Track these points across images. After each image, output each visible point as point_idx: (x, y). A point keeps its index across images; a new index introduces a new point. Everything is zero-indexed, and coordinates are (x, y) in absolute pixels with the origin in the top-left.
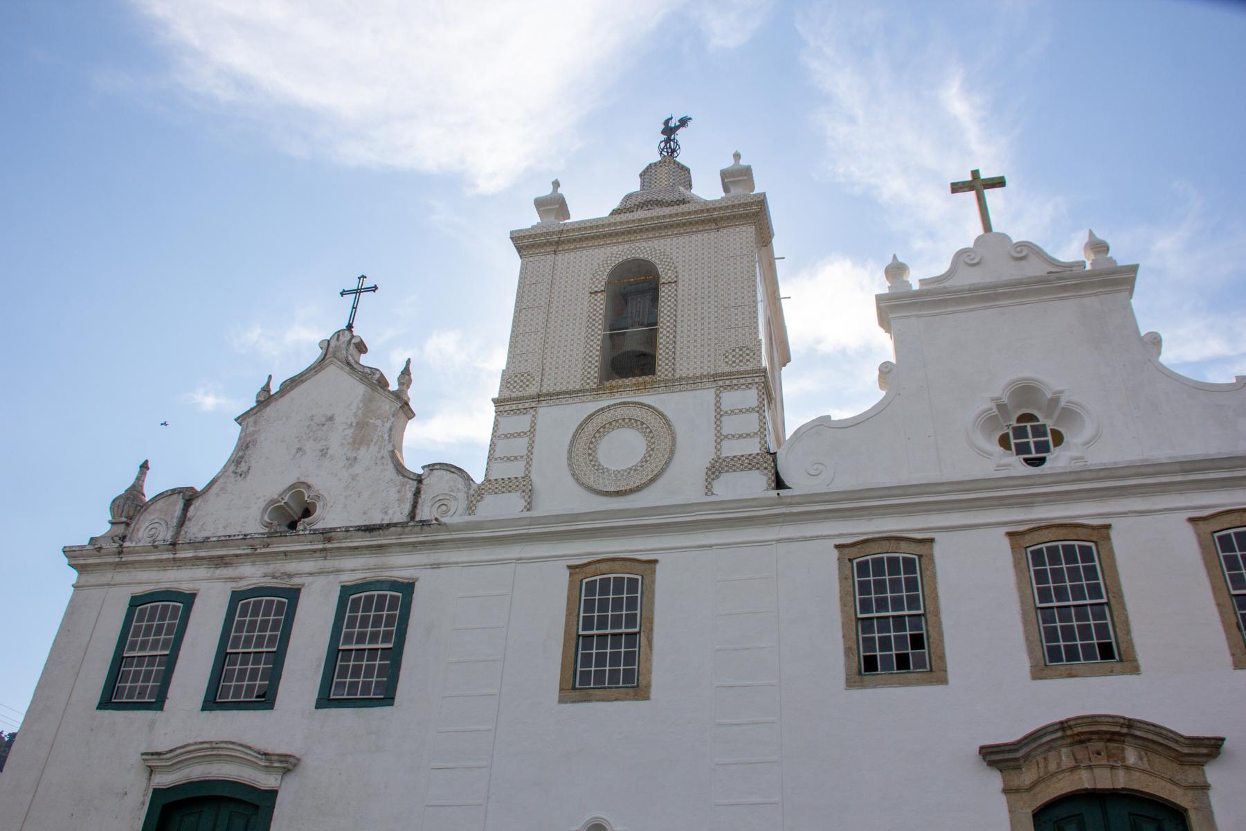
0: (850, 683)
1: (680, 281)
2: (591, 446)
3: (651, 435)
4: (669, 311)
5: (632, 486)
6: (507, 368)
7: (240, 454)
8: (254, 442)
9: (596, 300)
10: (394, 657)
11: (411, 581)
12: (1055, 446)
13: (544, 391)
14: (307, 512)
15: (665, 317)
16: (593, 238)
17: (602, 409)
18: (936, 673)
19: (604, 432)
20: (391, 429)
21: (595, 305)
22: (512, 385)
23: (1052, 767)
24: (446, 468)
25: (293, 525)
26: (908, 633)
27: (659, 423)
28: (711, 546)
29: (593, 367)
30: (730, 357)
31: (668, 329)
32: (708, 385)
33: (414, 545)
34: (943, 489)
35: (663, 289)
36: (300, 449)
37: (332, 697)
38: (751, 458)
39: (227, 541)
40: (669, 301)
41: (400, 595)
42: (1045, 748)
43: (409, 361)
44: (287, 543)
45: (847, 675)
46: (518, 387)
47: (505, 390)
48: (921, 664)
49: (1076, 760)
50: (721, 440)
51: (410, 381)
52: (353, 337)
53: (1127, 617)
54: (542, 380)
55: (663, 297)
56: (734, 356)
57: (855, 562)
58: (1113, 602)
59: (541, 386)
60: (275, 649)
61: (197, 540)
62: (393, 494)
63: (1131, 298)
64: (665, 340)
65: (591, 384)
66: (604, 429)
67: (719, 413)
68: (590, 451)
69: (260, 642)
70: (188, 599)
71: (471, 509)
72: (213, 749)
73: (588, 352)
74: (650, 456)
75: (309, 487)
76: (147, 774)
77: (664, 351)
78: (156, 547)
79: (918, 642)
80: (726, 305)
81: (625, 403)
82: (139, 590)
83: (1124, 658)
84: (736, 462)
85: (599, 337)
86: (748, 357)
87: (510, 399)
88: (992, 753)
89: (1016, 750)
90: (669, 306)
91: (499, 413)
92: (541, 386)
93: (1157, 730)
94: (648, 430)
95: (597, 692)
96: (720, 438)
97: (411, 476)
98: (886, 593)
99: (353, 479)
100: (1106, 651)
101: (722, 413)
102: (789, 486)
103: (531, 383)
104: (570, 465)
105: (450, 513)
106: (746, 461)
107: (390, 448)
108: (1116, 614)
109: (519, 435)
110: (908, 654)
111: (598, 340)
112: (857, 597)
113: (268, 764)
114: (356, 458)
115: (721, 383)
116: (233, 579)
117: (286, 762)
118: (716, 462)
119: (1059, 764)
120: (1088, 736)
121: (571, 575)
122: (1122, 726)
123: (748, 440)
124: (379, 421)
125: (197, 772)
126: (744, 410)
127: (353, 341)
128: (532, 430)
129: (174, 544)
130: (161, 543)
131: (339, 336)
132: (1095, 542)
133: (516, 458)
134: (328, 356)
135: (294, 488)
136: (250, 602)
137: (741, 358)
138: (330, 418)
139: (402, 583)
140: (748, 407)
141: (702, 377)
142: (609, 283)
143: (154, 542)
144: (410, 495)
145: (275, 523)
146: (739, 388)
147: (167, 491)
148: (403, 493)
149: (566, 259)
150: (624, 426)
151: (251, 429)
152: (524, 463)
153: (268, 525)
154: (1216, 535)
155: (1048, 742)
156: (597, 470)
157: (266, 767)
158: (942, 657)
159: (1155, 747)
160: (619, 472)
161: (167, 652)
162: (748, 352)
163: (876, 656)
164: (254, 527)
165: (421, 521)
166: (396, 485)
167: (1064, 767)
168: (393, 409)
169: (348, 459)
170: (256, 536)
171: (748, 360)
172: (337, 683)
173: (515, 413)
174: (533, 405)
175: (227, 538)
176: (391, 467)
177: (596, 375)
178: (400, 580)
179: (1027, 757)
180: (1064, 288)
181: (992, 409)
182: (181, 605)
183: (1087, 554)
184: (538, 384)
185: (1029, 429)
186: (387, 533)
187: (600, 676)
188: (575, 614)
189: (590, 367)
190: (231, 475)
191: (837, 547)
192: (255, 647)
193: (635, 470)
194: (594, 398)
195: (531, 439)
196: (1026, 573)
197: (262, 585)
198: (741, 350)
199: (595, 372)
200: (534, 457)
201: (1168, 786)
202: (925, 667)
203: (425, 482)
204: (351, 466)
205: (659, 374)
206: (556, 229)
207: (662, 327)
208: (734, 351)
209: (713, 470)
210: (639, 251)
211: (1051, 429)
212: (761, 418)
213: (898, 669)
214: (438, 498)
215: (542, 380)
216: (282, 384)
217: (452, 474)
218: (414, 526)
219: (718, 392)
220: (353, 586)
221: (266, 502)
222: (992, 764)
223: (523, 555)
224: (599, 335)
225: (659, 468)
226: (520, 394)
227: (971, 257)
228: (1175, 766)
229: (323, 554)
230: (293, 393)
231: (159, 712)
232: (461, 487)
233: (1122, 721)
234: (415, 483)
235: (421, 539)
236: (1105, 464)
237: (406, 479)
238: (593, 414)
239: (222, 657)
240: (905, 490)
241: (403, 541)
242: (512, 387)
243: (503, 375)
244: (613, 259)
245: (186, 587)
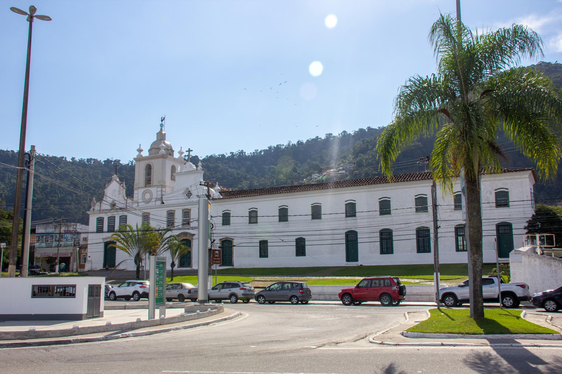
82: (98, 217)
96: (157, 195)
245: (103, 217)
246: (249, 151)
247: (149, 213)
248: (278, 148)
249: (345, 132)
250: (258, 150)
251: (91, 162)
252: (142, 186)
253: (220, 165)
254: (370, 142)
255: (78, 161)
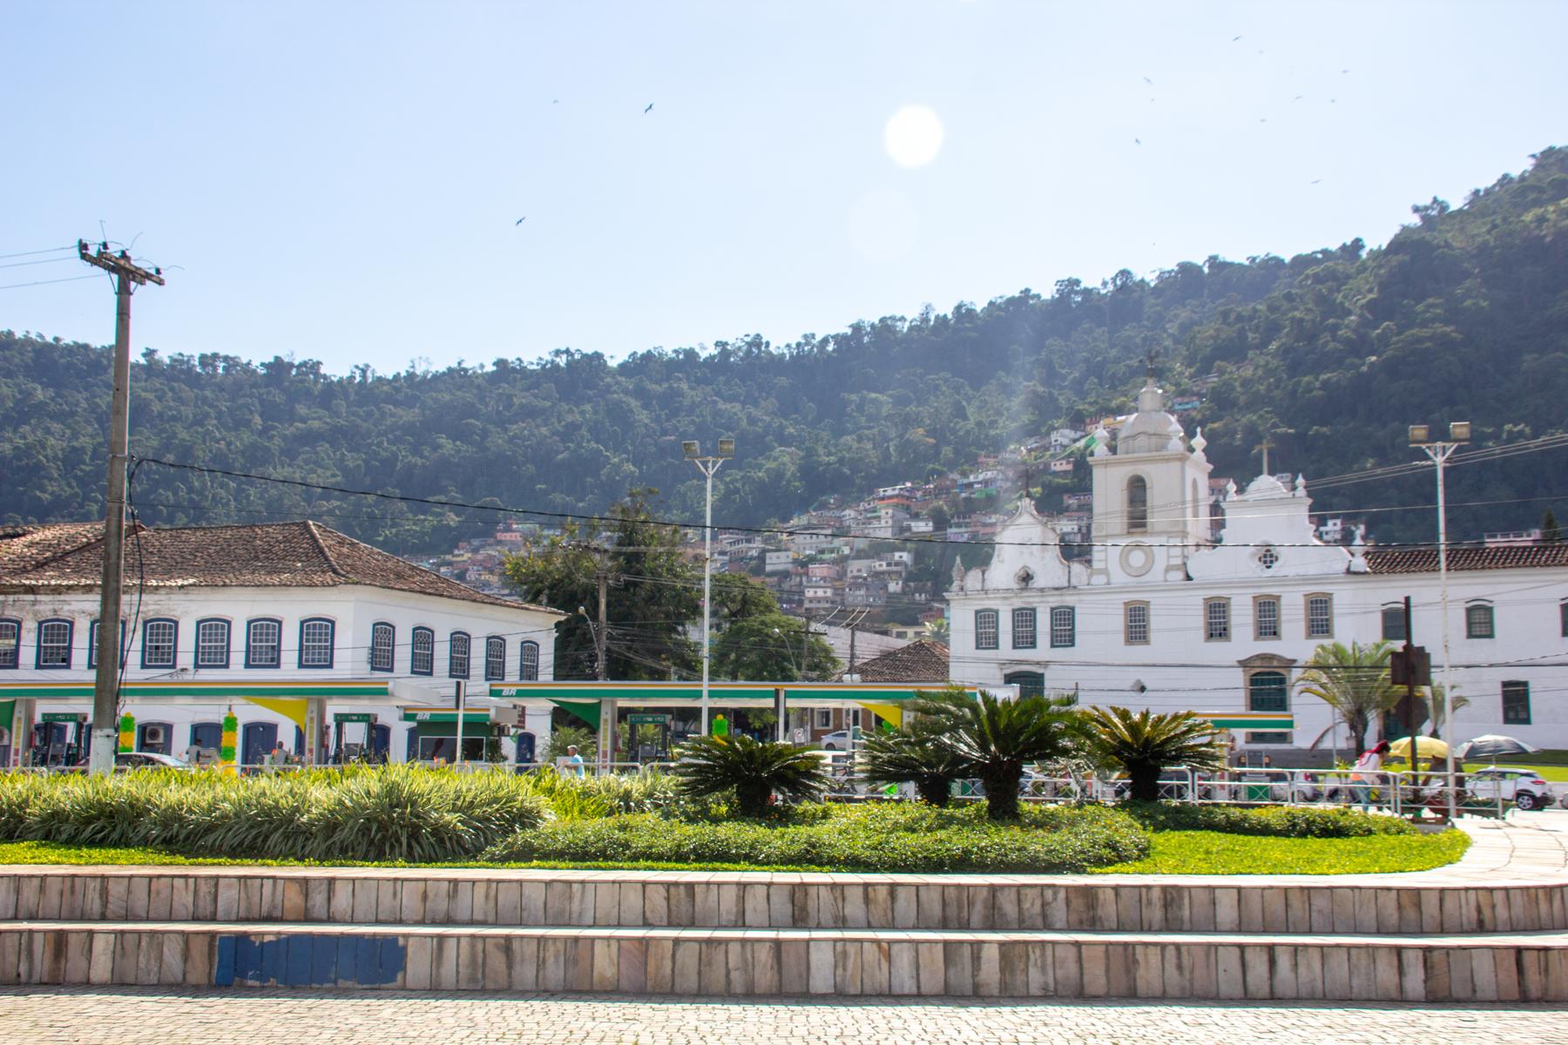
82: (979, 608)
100: (1275, 633)
245: (995, 607)
246: (781, 339)
247: (1148, 603)
248: (885, 328)
249: (1125, 273)
250: (813, 336)
251: (215, 368)
252: (1118, 531)
253: (684, 386)
254: (1251, 318)
255: (167, 361)
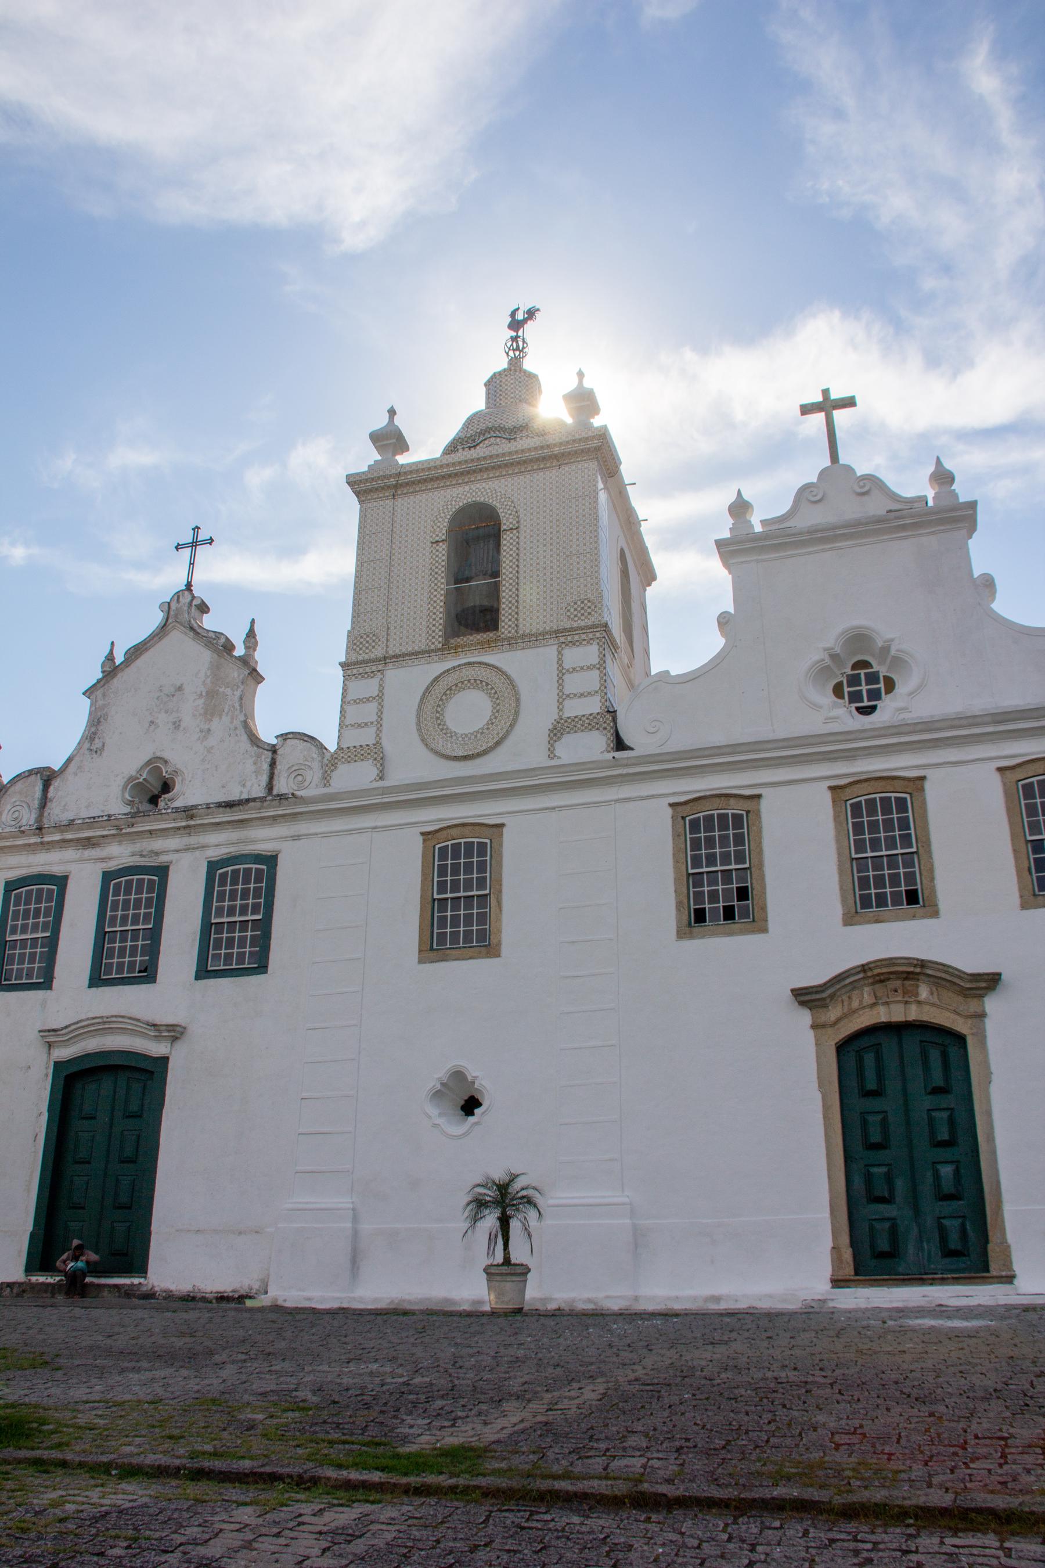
0: (681, 935)
1: (522, 527)
2: (439, 709)
3: (496, 696)
4: (511, 561)
5: (479, 750)
6: (353, 628)
7: (93, 729)
8: (106, 717)
9: (437, 551)
10: (265, 927)
11: (274, 854)
12: (886, 693)
13: (391, 653)
14: (166, 787)
15: (508, 567)
16: (432, 479)
17: (448, 670)
18: (758, 924)
19: (451, 694)
20: (241, 699)
21: (437, 556)
22: (358, 646)
23: (855, 1004)
24: (299, 737)
25: (154, 800)
26: (735, 886)
27: (504, 683)
28: (554, 808)
29: (437, 624)
30: (572, 610)
31: (511, 581)
32: (551, 642)
33: (274, 818)
34: (769, 746)
35: (505, 537)
36: (152, 722)
37: (209, 968)
38: (591, 718)
39: (93, 822)
40: (511, 550)
41: (264, 867)
42: (849, 988)
43: (253, 622)
44: (150, 822)
45: (678, 927)
46: (364, 648)
47: (352, 653)
48: (745, 914)
49: (876, 997)
50: (564, 700)
51: (256, 643)
52: (193, 597)
53: (932, 865)
54: (388, 640)
55: (505, 545)
56: (575, 610)
57: (688, 819)
58: (921, 851)
59: (387, 646)
60: (150, 926)
61: (63, 823)
62: (249, 767)
63: (970, 537)
64: (507, 594)
65: (436, 643)
66: (451, 691)
67: (561, 672)
68: (438, 715)
69: (136, 920)
70: (62, 882)
71: (326, 779)
72: (104, 1023)
73: (431, 609)
74: (496, 718)
75: (166, 762)
76: (46, 1050)
77: (507, 606)
78: (23, 832)
79: (743, 893)
80: (568, 553)
81: (469, 663)
82: (13, 875)
83: (927, 904)
84: (577, 722)
85: (442, 592)
86: (589, 610)
87: (357, 663)
88: (801, 995)
89: (823, 991)
90: (511, 555)
91: (347, 678)
92: (387, 646)
93: (945, 969)
94: (493, 691)
95: (453, 952)
96: (562, 697)
97: (266, 747)
98: (715, 848)
99: (209, 751)
100: (912, 897)
101: (564, 671)
102: (632, 746)
103: (376, 643)
104: (419, 730)
105: (306, 784)
106: (587, 721)
107: (242, 718)
108: (922, 862)
109: (368, 700)
110: (734, 906)
111: (442, 595)
112: (689, 853)
113: (157, 1034)
114: (209, 730)
115: (562, 639)
116: (102, 860)
117: (174, 1031)
118: (558, 723)
119: (861, 1001)
120: (886, 976)
121: (424, 841)
122: (915, 966)
123: (589, 698)
124: (229, 689)
125: (92, 1044)
126: (585, 668)
127: (195, 603)
128: (381, 694)
129: (40, 829)
130: (27, 828)
131: (178, 597)
132: (910, 794)
133: (366, 724)
134: (170, 621)
135: (151, 764)
136: (121, 881)
137: (582, 612)
138: (179, 687)
139: (266, 856)
140: (589, 664)
141: (543, 634)
142: (450, 531)
143: (20, 827)
144: (266, 767)
145: (137, 800)
146: (581, 644)
147: (24, 772)
148: (259, 765)
149: (406, 504)
150: (469, 688)
151: (100, 703)
152: (375, 728)
153: (130, 803)
154: (1021, 783)
155: (851, 983)
156: (445, 734)
157: (156, 1036)
158: (764, 909)
159: (944, 983)
160: (466, 735)
161: (48, 934)
162: (589, 604)
163: (737, 888)
164: (118, 808)
165: (278, 795)
166: (251, 756)
167: (865, 1004)
168: (241, 677)
169: (201, 731)
170: (120, 816)
171: (589, 614)
172: (213, 955)
173: (363, 677)
174: (380, 667)
175: (92, 820)
176: (244, 737)
177: (441, 633)
178: (263, 853)
179: (832, 997)
180: (903, 527)
181: (823, 660)
182: (55, 887)
183: (902, 805)
184: (384, 645)
185: (863, 677)
186: (247, 808)
187: (455, 935)
188: (430, 879)
189: (434, 625)
190: (87, 752)
191: (671, 805)
192: (131, 925)
193: (482, 733)
194: (439, 658)
195: (380, 704)
196: (844, 825)
197: (132, 864)
198: (582, 602)
199: (440, 630)
200: (384, 723)
201: (953, 1016)
202: (749, 918)
203: (280, 752)
204: (205, 738)
205: (503, 630)
206: (393, 471)
207: (504, 580)
208: (575, 603)
209: (555, 731)
210: (479, 493)
211: (884, 676)
212: (602, 675)
213: (724, 920)
214: (294, 769)
215: (388, 640)
216: (126, 653)
217: (305, 743)
218: (273, 800)
219: (560, 649)
220: (218, 861)
221: (125, 780)
222: (802, 1003)
223: (379, 824)
224: (442, 589)
225: (505, 730)
226: (366, 657)
227: (814, 493)
228: (960, 999)
229: (187, 831)
230: (140, 662)
231: (49, 991)
232: (315, 756)
233: (915, 962)
234: (270, 754)
235: (280, 812)
236: (921, 718)
237: (261, 750)
238: (439, 676)
239: (101, 936)
240: (734, 748)
241: (263, 815)
242: (358, 649)
243: (348, 636)
244: (454, 503)
245: (57, 870)
